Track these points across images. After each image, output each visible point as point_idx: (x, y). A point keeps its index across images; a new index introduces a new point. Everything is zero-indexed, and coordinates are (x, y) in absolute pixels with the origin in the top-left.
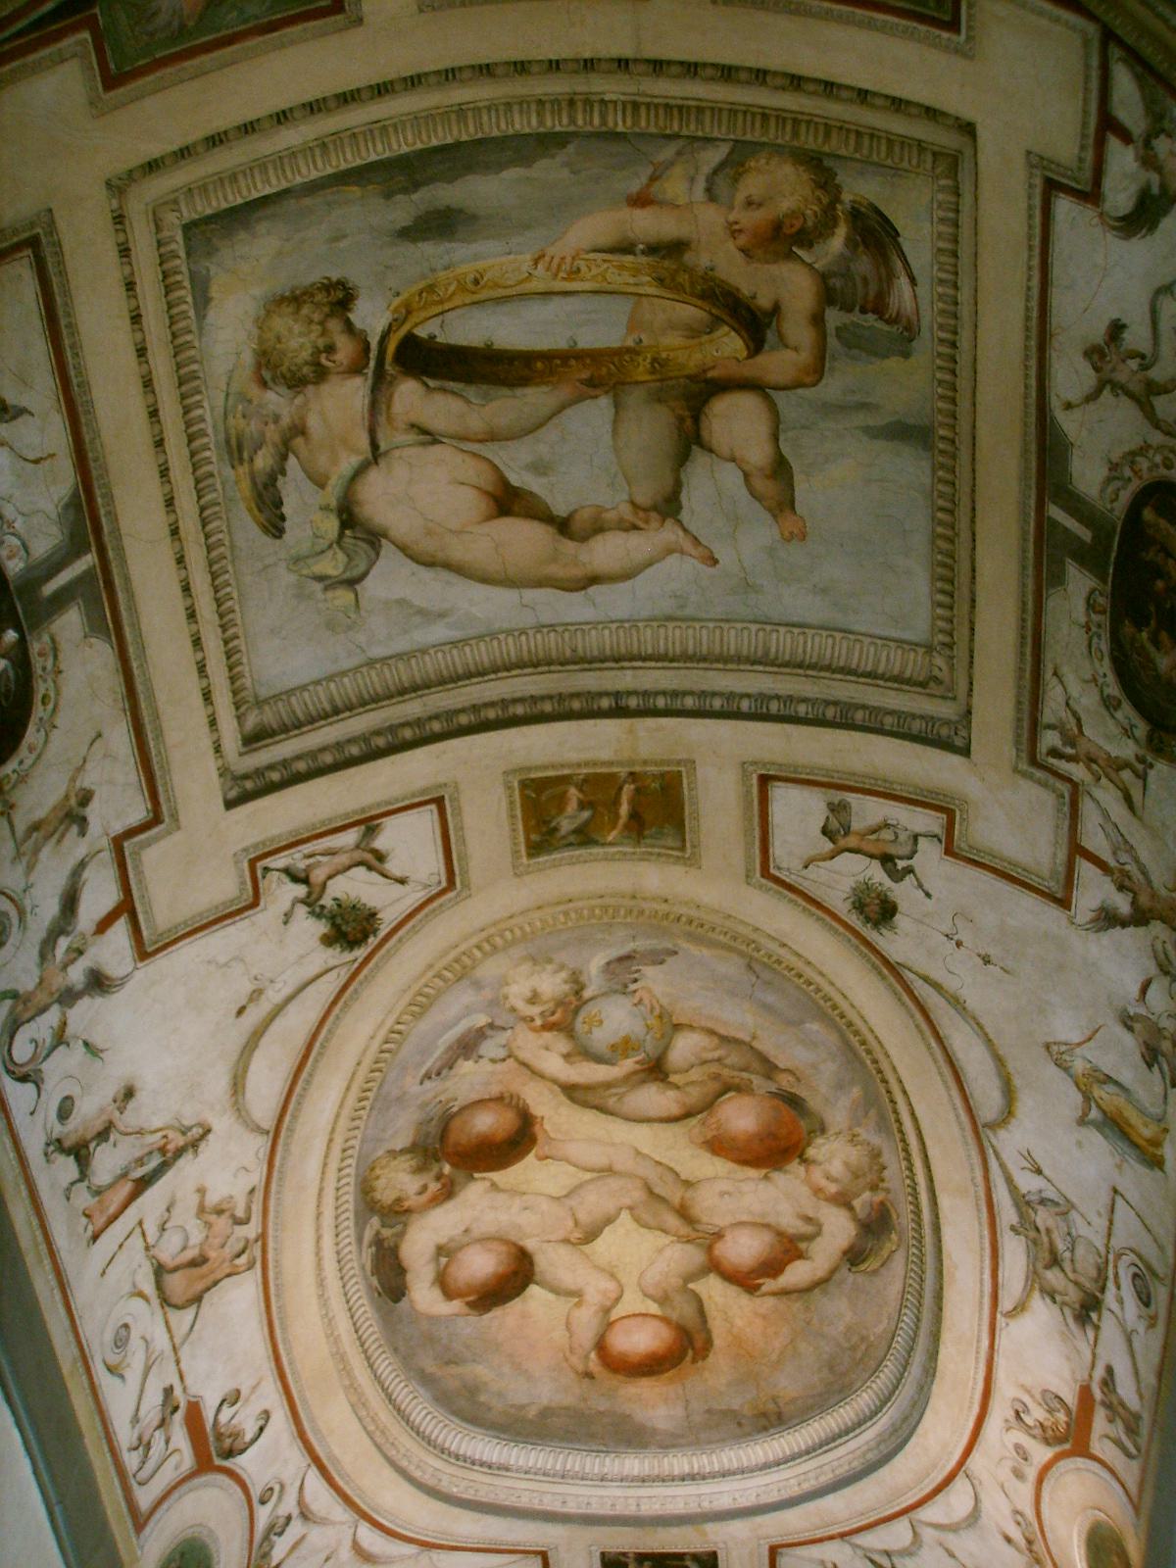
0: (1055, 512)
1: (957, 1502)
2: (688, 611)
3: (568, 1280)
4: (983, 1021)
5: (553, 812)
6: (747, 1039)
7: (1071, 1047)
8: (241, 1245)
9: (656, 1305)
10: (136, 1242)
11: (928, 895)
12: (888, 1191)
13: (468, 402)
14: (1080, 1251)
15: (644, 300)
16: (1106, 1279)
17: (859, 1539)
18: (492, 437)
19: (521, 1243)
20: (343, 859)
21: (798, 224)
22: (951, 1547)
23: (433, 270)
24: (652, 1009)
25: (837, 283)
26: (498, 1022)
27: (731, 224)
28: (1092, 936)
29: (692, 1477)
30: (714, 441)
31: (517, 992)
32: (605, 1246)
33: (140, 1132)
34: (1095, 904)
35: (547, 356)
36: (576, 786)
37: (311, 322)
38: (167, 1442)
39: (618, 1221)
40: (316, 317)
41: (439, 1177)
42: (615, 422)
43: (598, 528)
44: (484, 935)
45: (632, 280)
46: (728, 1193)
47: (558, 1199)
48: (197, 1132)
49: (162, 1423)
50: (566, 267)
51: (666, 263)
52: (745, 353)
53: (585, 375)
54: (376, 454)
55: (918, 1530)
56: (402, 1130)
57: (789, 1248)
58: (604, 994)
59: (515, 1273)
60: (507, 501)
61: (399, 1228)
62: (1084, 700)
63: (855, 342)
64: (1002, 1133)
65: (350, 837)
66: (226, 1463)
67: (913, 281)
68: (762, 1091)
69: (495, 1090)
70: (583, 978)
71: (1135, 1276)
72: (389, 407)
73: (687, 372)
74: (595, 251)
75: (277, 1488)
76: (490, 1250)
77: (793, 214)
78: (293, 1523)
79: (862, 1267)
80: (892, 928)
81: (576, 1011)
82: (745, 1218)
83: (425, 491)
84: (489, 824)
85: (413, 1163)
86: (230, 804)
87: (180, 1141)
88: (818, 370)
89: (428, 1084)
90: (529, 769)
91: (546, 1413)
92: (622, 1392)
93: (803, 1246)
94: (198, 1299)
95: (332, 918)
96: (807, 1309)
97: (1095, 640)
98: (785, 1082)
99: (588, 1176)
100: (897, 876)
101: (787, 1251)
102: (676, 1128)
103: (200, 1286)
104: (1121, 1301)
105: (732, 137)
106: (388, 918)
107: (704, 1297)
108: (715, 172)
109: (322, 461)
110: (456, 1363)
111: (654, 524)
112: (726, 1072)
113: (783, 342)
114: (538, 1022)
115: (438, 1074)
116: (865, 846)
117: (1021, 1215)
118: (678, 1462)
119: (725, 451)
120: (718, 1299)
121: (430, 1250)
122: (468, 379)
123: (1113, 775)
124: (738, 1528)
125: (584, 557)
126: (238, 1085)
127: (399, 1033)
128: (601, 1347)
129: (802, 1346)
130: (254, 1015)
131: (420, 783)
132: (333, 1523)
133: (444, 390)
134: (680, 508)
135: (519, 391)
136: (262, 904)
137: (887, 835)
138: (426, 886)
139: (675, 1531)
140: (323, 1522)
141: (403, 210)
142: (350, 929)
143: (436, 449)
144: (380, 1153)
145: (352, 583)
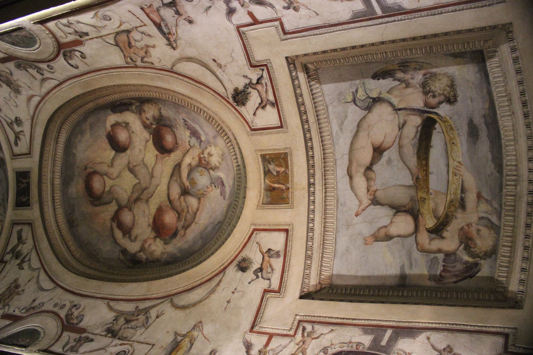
0: (389, 332)
1: (47, 284)
2: (340, 207)
3: (117, 163)
4: (207, 300)
5: (276, 163)
6: (196, 221)
7: (201, 331)
8: (134, 59)
10: (139, 23)
11: (249, 283)
13: (413, 139)
14: (131, 331)
15: (445, 196)
16: (123, 340)
17: (34, 251)
18: (400, 147)
20: (264, 95)
21: (472, 246)
23: (458, 130)
24: (206, 192)
25: (453, 257)
26: (202, 143)
27: (471, 225)
28: (241, 340)
30: (398, 217)
31: (212, 150)
32: (127, 174)
33: (177, 25)
34: (253, 341)
35: (427, 165)
37: (444, 90)
38: (70, 34)
40: (445, 92)
41: (151, 124)
42: (404, 186)
43: (368, 179)
44: (233, 140)
45: (452, 192)
47: (143, 160)
48: (174, 45)
49: (76, 32)
50: (457, 172)
51: (458, 203)
52: (427, 227)
53: (420, 177)
54: (397, 110)
56: (168, 112)
57: (127, 231)
58: (211, 176)
59: (119, 147)
60: (378, 151)
61: (135, 111)
62: (324, 340)
63: (433, 262)
64: (169, 305)
65: (271, 98)
66: (61, 55)
67: (455, 282)
68: (178, 225)
69: (180, 142)
70: (216, 170)
71: (125, 352)
72: (413, 114)
73: (421, 208)
74: (462, 181)
75: (52, 71)
77: (475, 244)
79: (121, 255)
80: (237, 271)
81: (206, 168)
82: (136, 218)
83: (383, 125)
84: (273, 142)
86: (287, 58)
87: (172, 40)
88: (423, 251)
89: (182, 121)
90: (291, 156)
91: (74, 155)
93: (127, 236)
94: (117, 45)
95: (244, 91)
97: (347, 345)
98: (182, 232)
99: (150, 170)
100: (255, 272)
102: (166, 198)
103: (121, 45)
104: (115, 346)
105: (502, 226)
106: (242, 109)
107: (111, 205)
108: (489, 220)
109: (396, 93)
111: (369, 197)
112: (184, 214)
113: (431, 240)
114: (202, 156)
115: (186, 124)
116: (265, 262)
117: (142, 310)
118: (58, 195)
119: (394, 220)
121: (128, 121)
122: (420, 140)
123: (300, 350)
125: (359, 174)
126: (189, 59)
127: (200, 112)
128: (95, 172)
131: (288, 121)
132: (40, 89)
133: (417, 132)
134: (375, 205)
135: (415, 156)
136: (252, 68)
137: (269, 270)
140: (41, 86)
141: (478, 121)
142: (239, 97)
143: (398, 129)
144: (160, 106)
145: (354, 101)
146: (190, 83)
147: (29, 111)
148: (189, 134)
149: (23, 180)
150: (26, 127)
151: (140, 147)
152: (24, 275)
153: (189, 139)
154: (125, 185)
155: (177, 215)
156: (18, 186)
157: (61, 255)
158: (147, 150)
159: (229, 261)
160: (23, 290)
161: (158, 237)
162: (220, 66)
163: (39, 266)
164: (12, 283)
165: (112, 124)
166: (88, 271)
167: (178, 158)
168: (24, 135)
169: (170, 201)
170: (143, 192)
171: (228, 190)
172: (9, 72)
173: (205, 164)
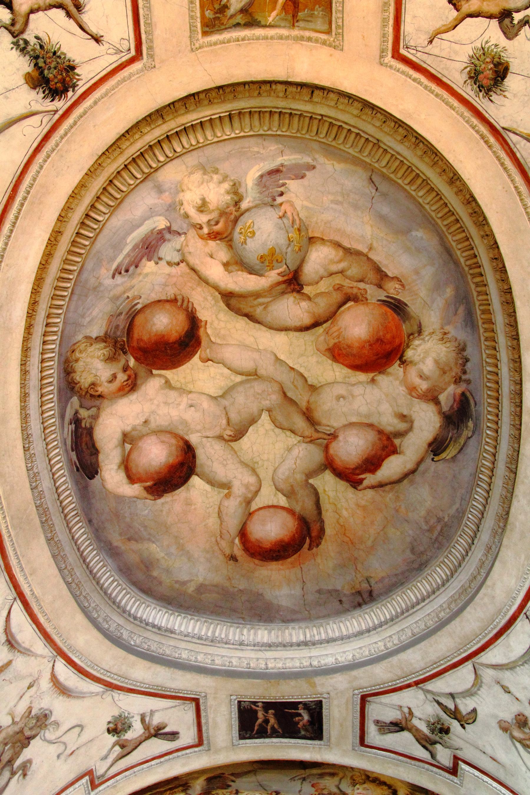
6: (365, 251)
9: (284, 498)
12: (468, 382)
17: (430, 686)
19: (187, 438)
22: (506, 683)
24: (293, 221)
26: (174, 228)
29: (305, 644)
31: (190, 198)
39: (260, 422)
41: (125, 369)
46: (343, 397)
47: (215, 398)
55: (479, 672)
56: (96, 319)
57: (387, 445)
58: (256, 206)
59: (181, 464)
61: (93, 411)
68: (374, 301)
69: (170, 292)
70: (242, 190)
76: (163, 442)
79: (443, 455)
81: (236, 221)
82: (354, 419)
85: (106, 352)
89: (119, 279)
91: (201, 588)
92: (257, 574)
93: (397, 441)
99: (239, 378)
101: (384, 448)
102: (307, 336)
107: (320, 491)
110: (136, 541)
112: (347, 283)
114: (206, 230)
115: (127, 271)
118: (295, 633)
120: (331, 494)
121: (118, 436)
124: (340, 682)
128: (243, 534)
129: (392, 532)
132: (35, 655)
138: (119, 51)
139: (293, 683)
140: (26, 652)
142: (52, 76)
144: (80, 337)
146: (17, 218)
147: (92, 694)
148: (152, 263)
149: (260, 721)
150: (134, 706)
151: (182, 406)
152: (492, 706)
153: (163, 263)
154: (275, 453)
156: (275, 734)
157: (442, 614)
158: (190, 387)
159: (475, 121)
161: (400, 359)
163: (468, 666)
165: (125, 480)
166: (485, 536)
167: (210, 298)
168: (152, 712)
169: (316, 324)
171: (289, 158)
173: (226, 222)
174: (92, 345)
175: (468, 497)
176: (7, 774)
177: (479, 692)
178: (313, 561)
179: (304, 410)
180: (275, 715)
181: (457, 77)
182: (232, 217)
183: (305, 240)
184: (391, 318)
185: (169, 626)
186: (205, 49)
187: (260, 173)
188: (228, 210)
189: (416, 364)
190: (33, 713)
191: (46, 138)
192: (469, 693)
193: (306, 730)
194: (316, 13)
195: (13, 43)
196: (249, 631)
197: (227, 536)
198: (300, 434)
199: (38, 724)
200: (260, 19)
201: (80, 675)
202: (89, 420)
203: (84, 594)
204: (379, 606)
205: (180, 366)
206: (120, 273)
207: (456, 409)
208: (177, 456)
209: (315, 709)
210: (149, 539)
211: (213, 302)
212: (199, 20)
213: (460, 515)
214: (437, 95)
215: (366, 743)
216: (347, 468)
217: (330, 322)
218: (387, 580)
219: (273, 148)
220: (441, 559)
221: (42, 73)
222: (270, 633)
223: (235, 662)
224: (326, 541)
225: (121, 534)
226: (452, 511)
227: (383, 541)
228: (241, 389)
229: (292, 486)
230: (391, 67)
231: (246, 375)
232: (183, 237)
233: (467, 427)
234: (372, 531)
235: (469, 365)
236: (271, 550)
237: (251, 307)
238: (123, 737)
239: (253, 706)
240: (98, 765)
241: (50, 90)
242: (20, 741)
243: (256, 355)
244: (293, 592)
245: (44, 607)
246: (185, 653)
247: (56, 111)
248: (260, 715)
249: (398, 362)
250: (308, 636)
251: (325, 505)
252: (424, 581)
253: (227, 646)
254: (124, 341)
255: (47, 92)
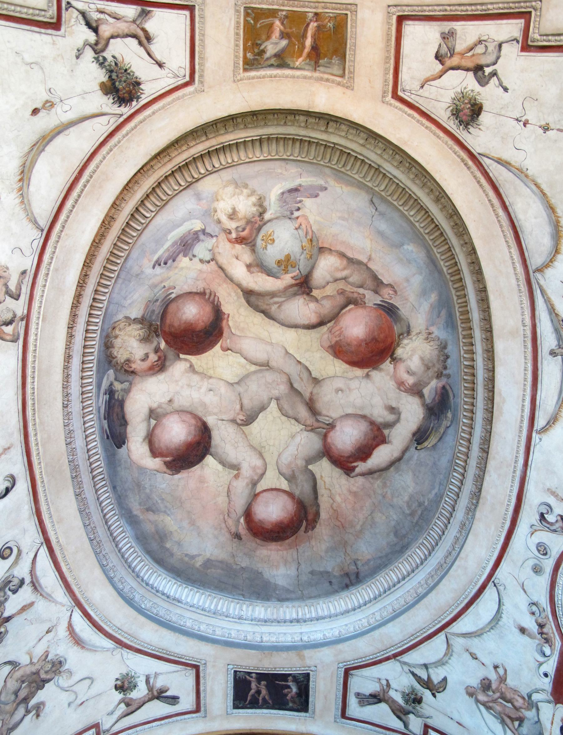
4: (539, 181)
5: (264, 37)
6: (365, 261)
8: (9, 316)
9: (286, 482)
11: (506, 90)
12: (448, 376)
17: (406, 658)
19: (205, 419)
20: (123, 27)
24: (307, 233)
26: (208, 231)
31: (223, 207)
36: (280, 20)
39: (269, 409)
41: (157, 350)
46: (342, 390)
47: (232, 384)
55: (451, 642)
57: (377, 435)
58: (277, 218)
59: (198, 443)
61: (127, 384)
68: (371, 304)
69: (200, 286)
70: (266, 204)
76: (183, 421)
78: (25, 587)
79: (426, 444)
81: (259, 229)
82: (350, 411)
85: (141, 332)
89: (158, 270)
91: (208, 563)
92: (258, 553)
93: (386, 432)
96: (385, 485)
99: (253, 368)
100: (483, 81)
101: (374, 438)
102: (314, 334)
106: (149, 91)
107: (318, 477)
110: (153, 511)
112: (349, 288)
114: (234, 235)
115: (165, 263)
118: (289, 611)
120: (327, 480)
121: (146, 411)
126: (25, 174)
128: (248, 514)
130: (47, 121)
137: (480, 49)
139: (284, 655)
142: (121, 87)
144: (120, 316)
146: (79, 196)
147: (104, 650)
148: (187, 259)
149: (252, 692)
151: (203, 390)
152: (461, 674)
153: (196, 260)
155: (351, 306)
156: (265, 705)
158: (211, 372)
159: (457, 148)
160: (496, 667)
162: (49, 105)
163: (441, 636)
164: (477, 701)
165: (148, 453)
166: (460, 515)
167: (233, 294)
168: (156, 675)
169: (321, 324)
170: (298, 393)
171: (307, 180)
172: (8, 668)
173: (251, 230)
174: (130, 325)
175: (445, 481)
176: (21, 711)
177: (450, 661)
178: (308, 543)
179: (307, 400)
180: (267, 686)
181: (442, 114)
182: (257, 225)
183: (316, 250)
184: (384, 319)
185: (177, 596)
186: (245, 81)
187: (282, 191)
188: (253, 220)
189: (404, 361)
190: (50, 658)
191: (111, 135)
192: (441, 663)
193: (294, 702)
194: (333, 61)
195: (94, 58)
196: (248, 607)
197: (233, 515)
198: (302, 423)
199: (54, 669)
200: (289, 62)
201: (94, 629)
202: (122, 393)
203: (104, 553)
204: (364, 586)
205: (203, 353)
206: (160, 265)
207: (437, 401)
208: (195, 436)
209: (303, 681)
210: (165, 512)
211: (235, 298)
212: (241, 59)
213: (439, 498)
214: (427, 128)
215: (347, 715)
216: (341, 456)
217: (333, 322)
218: (372, 562)
219: (293, 171)
220: (420, 541)
221: (114, 84)
222: (266, 610)
223: (234, 634)
224: (320, 524)
225: (140, 504)
226: (431, 496)
227: (371, 526)
228: (254, 377)
229: (293, 471)
230: (391, 105)
231: (260, 366)
232: (214, 239)
233: (446, 417)
234: (361, 516)
235: (449, 361)
236: (271, 531)
237: (268, 305)
238: (128, 696)
239: (248, 677)
240: (104, 719)
241: (119, 98)
242: (36, 682)
243: (269, 348)
244: (289, 572)
245: (67, 557)
246: (189, 620)
247: (121, 115)
248: (254, 685)
249: (389, 359)
250: (300, 614)
251: (322, 491)
252: (405, 562)
253: (227, 619)
254: (158, 325)
255: (116, 99)
